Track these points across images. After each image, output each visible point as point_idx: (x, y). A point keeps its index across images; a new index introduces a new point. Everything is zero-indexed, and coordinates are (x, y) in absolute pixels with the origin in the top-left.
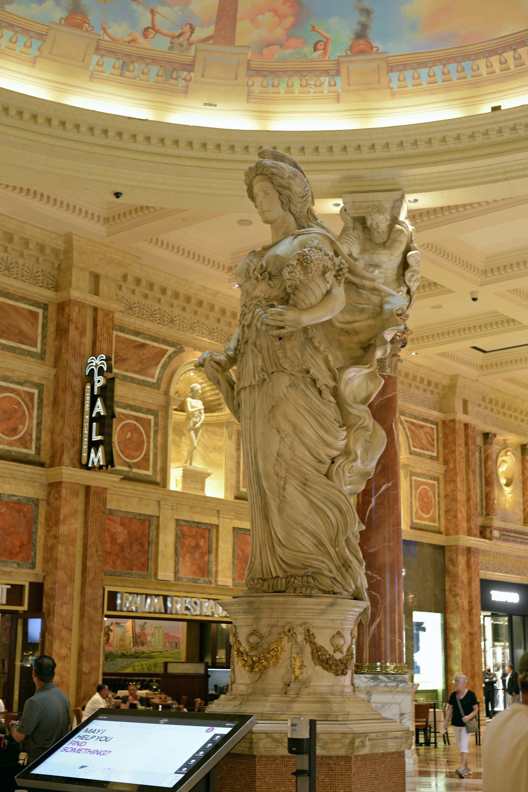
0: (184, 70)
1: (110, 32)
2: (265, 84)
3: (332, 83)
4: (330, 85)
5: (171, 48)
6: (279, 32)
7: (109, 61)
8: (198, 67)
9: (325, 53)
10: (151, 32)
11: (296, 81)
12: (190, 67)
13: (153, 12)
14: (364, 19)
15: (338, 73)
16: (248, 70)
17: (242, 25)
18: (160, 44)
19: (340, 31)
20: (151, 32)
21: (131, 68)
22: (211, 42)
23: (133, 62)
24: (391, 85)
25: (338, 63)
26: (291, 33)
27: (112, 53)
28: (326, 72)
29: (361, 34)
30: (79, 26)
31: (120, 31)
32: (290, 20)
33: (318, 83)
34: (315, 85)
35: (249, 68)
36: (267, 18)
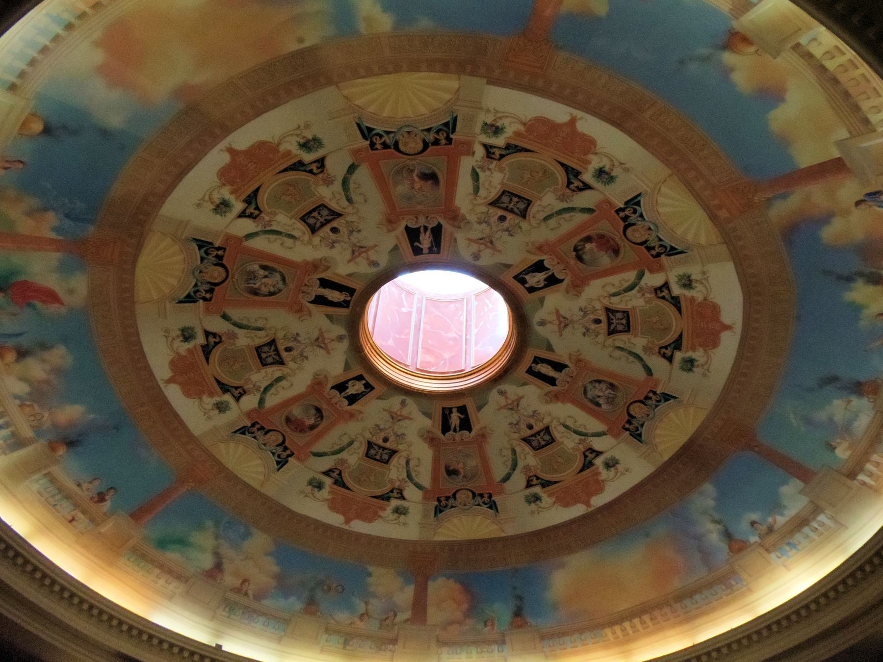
0: (390, 644)
1: (336, 617)
5: (380, 628)
6: (458, 615)
7: (334, 638)
8: (400, 642)
10: (366, 617)
11: (474, 650)
12: (394, 641)
13: (366, 603)
17: (431, 611)
18: (372, 626)
19: (502, 611)
20: (366, 617)
21: (351, 643)
23: (353, 639)
25: (503, 635)
27: (337, 632)
28: (496, 642)
30: (313, 614)
31: (343, 616)
35: (438, 641)
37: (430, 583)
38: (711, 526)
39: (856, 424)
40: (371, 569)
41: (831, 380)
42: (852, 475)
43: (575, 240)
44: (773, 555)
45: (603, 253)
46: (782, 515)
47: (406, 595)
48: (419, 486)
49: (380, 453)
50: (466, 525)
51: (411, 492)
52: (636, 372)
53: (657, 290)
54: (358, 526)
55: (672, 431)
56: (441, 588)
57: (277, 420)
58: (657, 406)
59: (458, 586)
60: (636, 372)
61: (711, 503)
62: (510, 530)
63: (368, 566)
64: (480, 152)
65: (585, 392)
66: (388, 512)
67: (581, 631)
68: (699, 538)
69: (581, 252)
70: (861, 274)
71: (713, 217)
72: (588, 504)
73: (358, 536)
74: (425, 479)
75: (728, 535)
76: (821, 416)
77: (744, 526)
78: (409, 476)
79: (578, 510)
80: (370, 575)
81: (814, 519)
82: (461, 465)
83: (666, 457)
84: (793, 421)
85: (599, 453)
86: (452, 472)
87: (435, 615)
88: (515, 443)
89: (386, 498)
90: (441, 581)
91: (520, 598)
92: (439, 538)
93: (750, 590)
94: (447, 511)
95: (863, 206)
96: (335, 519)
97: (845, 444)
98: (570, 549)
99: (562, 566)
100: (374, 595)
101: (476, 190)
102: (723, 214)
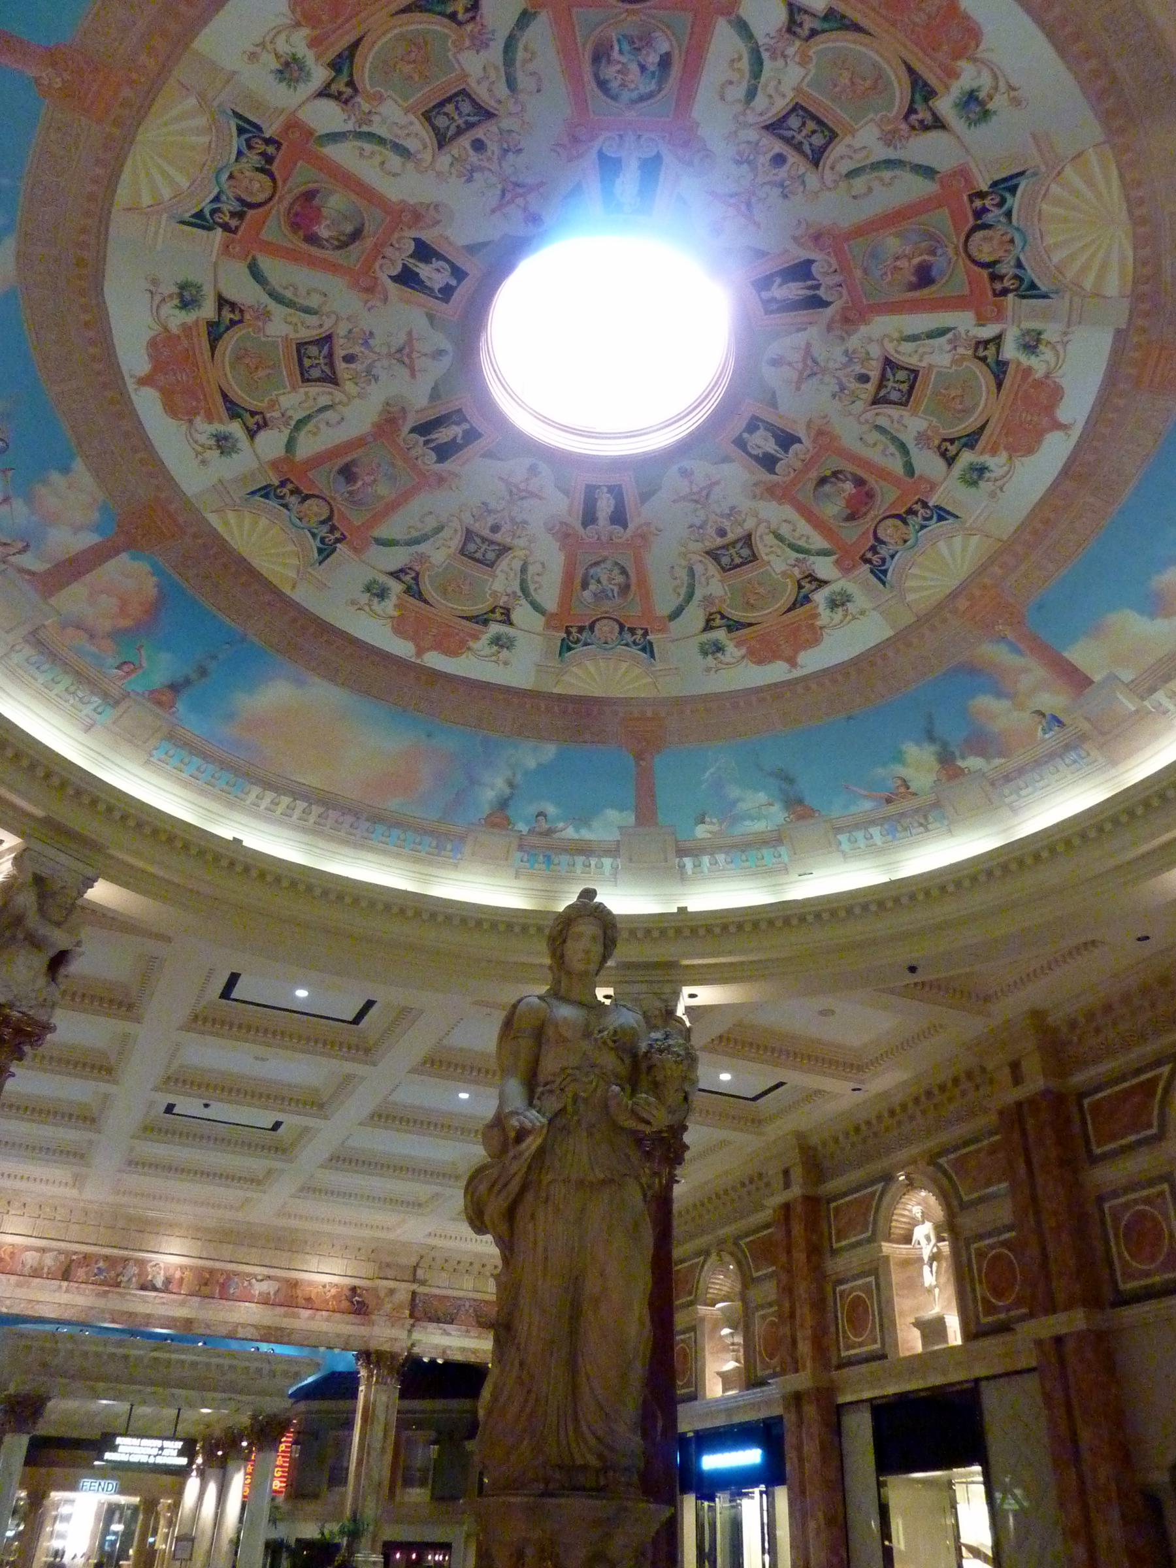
2: (33, 659)
3: (99, 710)
4: (95, 710)
6: (107, 625)
9: (125, 677)
11: (67, 681)
14: (193, 676)
15: (117, 703)
16: (30, 633)
19: (161, 667)
22: (27, 577)
24: (154, 752)
25: (126, 696)
26: (116, 635)
28: (105, 695)
29: (175, 688)
32: (127, 623)
33: (86, 699)
34: (80, 699)
35: (34, 633)
36: (108, 603)
37: (124, 557)
38: (500, 783)
39: (747, 823)
40: (78, 465)
41: (787, 778)
42: (682, 852)
43: (850, 467)
44: (519, 855)
45: (843, 503)
46: (577, 831)
47: (68, 540)
48: (290, 445)
49: (318, 360)
50: (268, 543)
51: (271, 443)
52: (664, 604)
53: (812, 578)
54: (148, 404)
55: (601, 674)
56: (130, 575)
57: (302, 176)
58: (627, 645)
59: (151, 592)
60: (664, 604)
61: (532, 764)
62: (302, 595)
63: (79, 460)
64: (988, 332)
65: (592, 566)
66: (205, 429)
67: (225, 765)
68: (473, 781)
69: (833, 479)
70: (945, 745)
71: (953, 596)
72: (420, 652)
73: (124, 410)
74: (307, 447)
75: (503, 804)
76: (734, 792)
77: (532, 810)
78: (301, 423)
79: (402, 648)
80: (66, 470)
81: (600, 856)
82: (368, 479)
83: (555, 691)
84: (708, 774)
85: (509, 622)
86: (348, 473)
87: (74, 599)
88: (455, 524)
89: (234, 410)
90: (141, 567)
91: (203, 672)
92: (214, 519)
93: (456, 866)
94: (272, 504)
95: (1037, 718)
96: (134, 359)
97: (715, 828)
98: (332, 675)
99: (300, 683)
100: (29, 499)
101: (914, 338)
102: (962, 604)
